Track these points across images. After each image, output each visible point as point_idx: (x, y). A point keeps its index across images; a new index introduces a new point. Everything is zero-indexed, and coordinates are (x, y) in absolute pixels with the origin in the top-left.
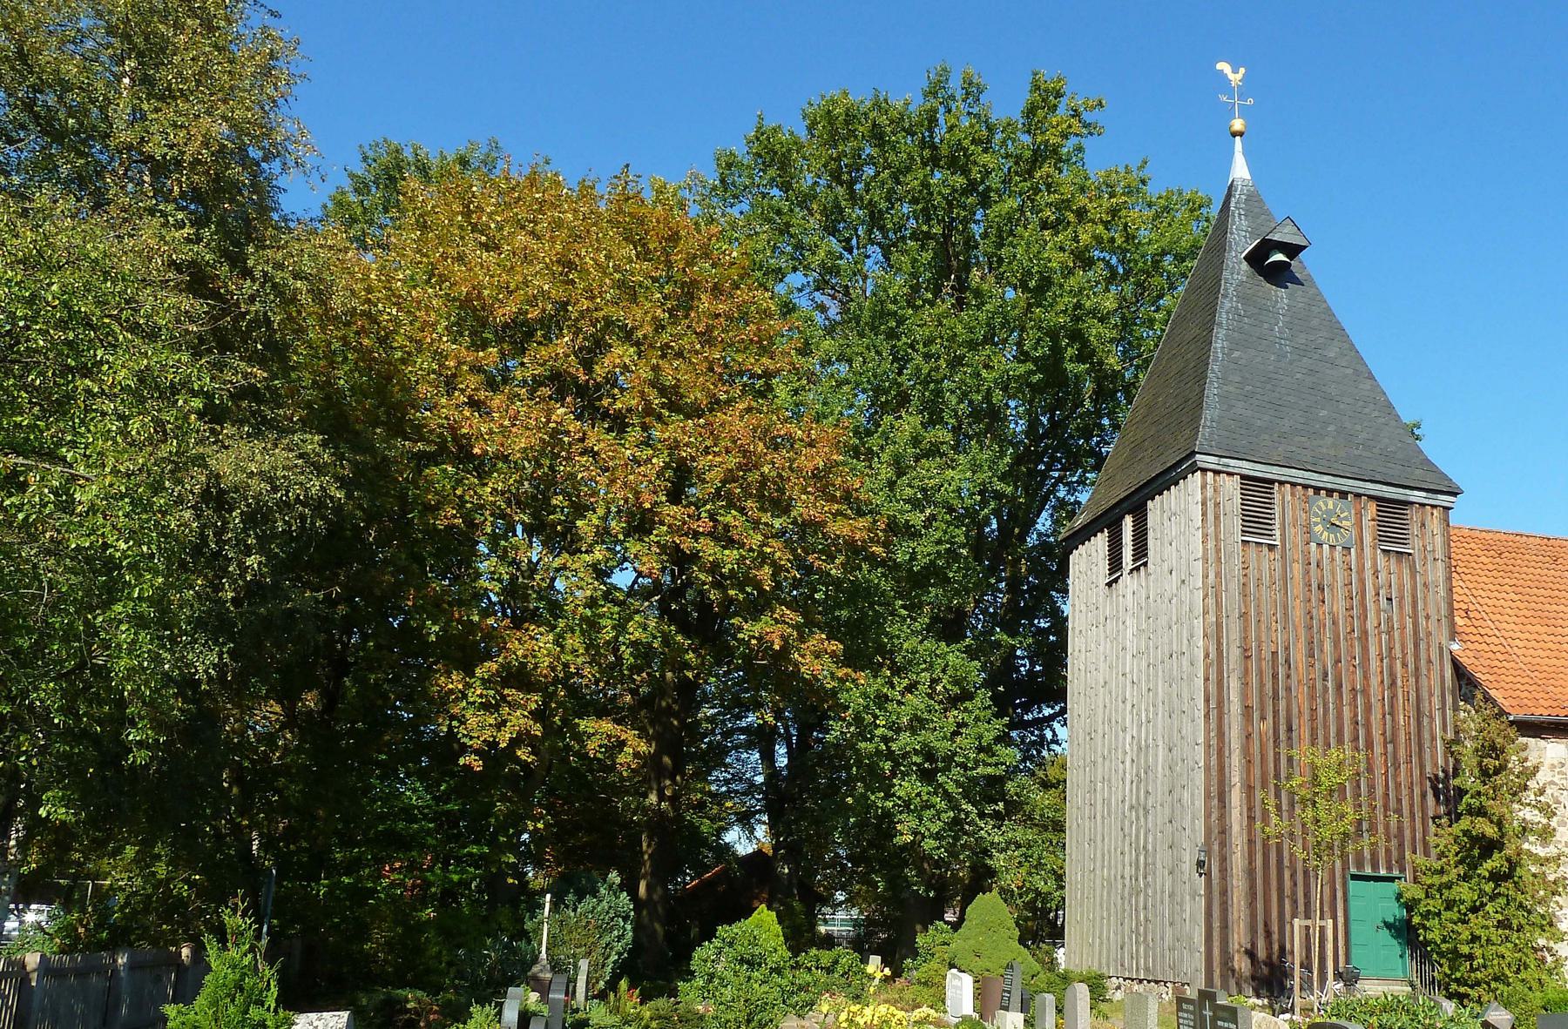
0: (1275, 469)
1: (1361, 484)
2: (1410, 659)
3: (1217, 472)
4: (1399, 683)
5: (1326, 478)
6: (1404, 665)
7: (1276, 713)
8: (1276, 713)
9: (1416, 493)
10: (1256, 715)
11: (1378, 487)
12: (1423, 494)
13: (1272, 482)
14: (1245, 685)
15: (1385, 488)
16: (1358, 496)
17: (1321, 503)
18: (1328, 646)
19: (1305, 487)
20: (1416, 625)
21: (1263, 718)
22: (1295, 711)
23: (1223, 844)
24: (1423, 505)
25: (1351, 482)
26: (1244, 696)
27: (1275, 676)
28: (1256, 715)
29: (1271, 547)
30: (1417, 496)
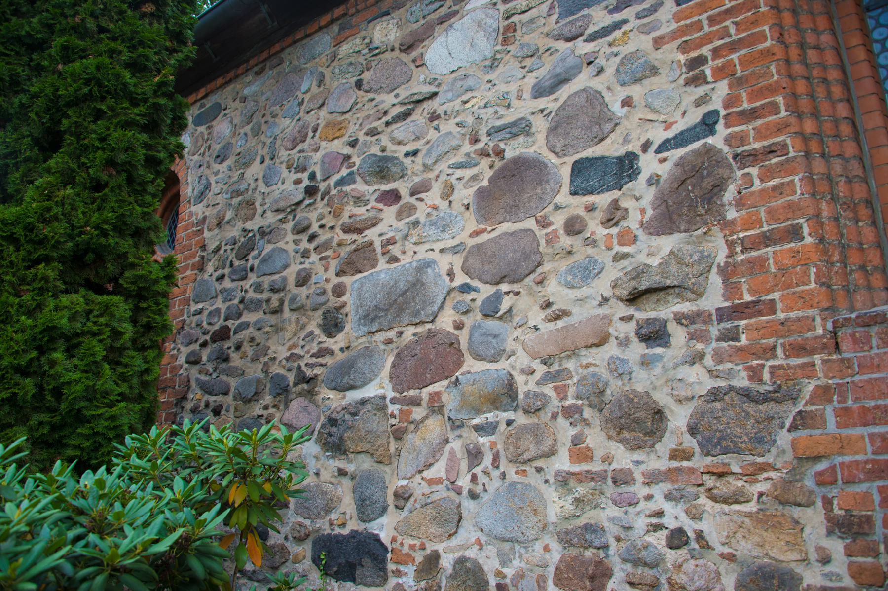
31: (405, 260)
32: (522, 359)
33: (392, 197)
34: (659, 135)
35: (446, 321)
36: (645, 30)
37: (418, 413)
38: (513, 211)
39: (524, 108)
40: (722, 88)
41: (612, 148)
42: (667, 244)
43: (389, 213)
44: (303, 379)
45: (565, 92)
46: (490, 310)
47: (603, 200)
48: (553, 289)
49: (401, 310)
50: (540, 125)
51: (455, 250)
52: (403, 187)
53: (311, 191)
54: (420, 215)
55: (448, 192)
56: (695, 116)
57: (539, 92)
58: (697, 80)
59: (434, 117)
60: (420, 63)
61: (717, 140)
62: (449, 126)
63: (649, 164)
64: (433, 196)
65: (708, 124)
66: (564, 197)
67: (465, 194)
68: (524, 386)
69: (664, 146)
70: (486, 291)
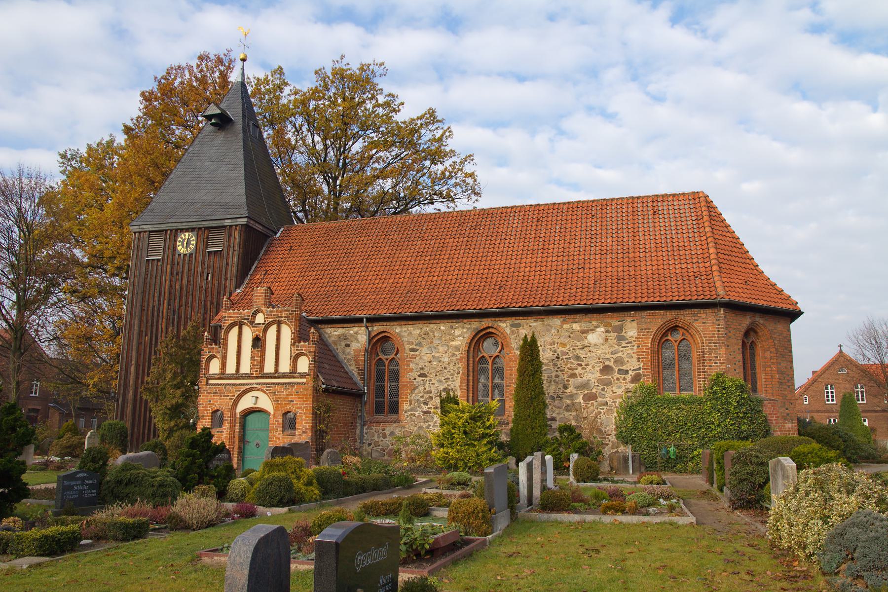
0: (162, 225)
1: (200, 223)
2: (215, 301)
3: (140, 233)
4: (209, 312)
5: (184, 224)
6: (212, 303)
7: (152, 332)
8: (152, 332)
9: (226, 221)
10: (144, 334)
11: (207, 222)
12: (230, 221)
13: (162, 231)
14: (141, 321)
15: (211, 222)
16: (200, 229)
17: (183, 236)
18: (177, 300)
19: (176, 230)
20: (220, 284)
21: (146, 335)
22: (160, 330)
23: (125, 389)
24: (231, 226)
25: (195, 223)
26: (140, 327)
27: (153, 316)
28: (144, 334)
29: (158, 260)
30: (227, 222)
31: (584, 378)
32: (608, 399)
33: (581, 365)
34: (632, 369)
35: (594, 391)
36: (632, 349)
37: (589, 406)
38: (607, 374)
39: (608, 356)
40: (642, 364)
41: (624, 368)
42: (633, 385)
43: (580, 368)
44: (558, 396)
45: (617, 355)
46: (603, 390)
47: (623, 376)
48: (614, 389)
49: (584, 387)
50: (612, 360)
51: (595, 378)
52: (583, 364)
53: (558, 358)
54: (588, 370)
55: (593, 367)
56: (638, 367)
57: (612, 353)
58: (639, 361)
59: (590, 351)
60: (586, 338)
61: (641, 371)
62: (594, 354)
63: (630, 372)
64: (590, 367)
65: (640, 369)
66: (616, 374)
67: (598, 369)
68: (609, 403)
69: (633, 370)
70: (602, 387)
